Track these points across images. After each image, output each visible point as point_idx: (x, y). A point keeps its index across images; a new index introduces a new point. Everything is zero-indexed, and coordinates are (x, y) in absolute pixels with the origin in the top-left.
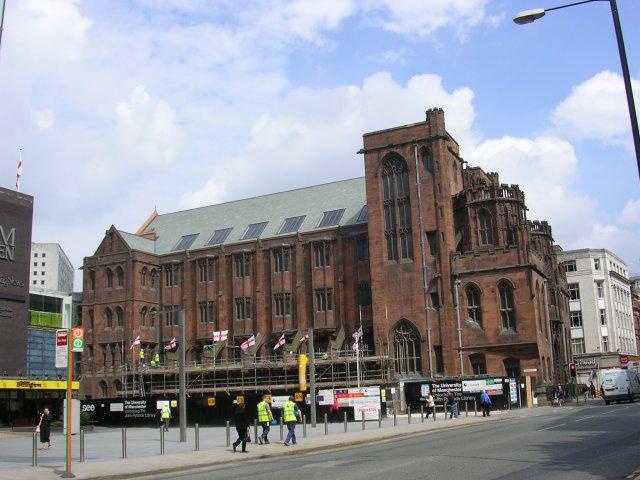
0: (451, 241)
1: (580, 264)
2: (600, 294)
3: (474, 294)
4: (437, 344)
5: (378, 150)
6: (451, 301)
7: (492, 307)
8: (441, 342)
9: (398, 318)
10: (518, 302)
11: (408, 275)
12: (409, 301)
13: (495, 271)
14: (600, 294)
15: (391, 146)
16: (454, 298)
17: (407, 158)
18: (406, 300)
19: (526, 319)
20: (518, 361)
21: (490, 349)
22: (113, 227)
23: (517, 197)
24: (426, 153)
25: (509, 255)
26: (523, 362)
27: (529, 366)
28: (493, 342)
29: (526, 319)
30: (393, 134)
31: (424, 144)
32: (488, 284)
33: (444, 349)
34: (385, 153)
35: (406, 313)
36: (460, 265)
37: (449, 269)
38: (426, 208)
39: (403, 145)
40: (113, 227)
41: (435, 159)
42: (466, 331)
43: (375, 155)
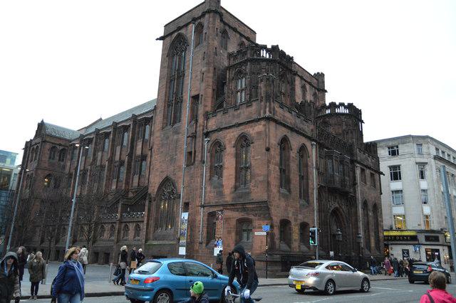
0: (207, 104)
1: (402, 149)
2: (422, 176)
3: (218, 147)
4: (187, 201)
7: (229, 163)
9: (164, 177)
11: (175, 137)
12: (173, 160)
13: (240, 125)
14: (422, 176)
19: (258, 175)
20: (249, 221)
21: (226, 206)
22: (42, 121)
23: (317, 83)
25: (250, 109)
26: (256, 223)
27: (260, 228)
28: (228, 198)
29: (258, 175)
30: (182, 19)
32: (230, 137)
34: (176, 34)
36: (212, 124)
37: (202, 128)
39: (186, 25)
40: (42, 121)
42: (208, 189)
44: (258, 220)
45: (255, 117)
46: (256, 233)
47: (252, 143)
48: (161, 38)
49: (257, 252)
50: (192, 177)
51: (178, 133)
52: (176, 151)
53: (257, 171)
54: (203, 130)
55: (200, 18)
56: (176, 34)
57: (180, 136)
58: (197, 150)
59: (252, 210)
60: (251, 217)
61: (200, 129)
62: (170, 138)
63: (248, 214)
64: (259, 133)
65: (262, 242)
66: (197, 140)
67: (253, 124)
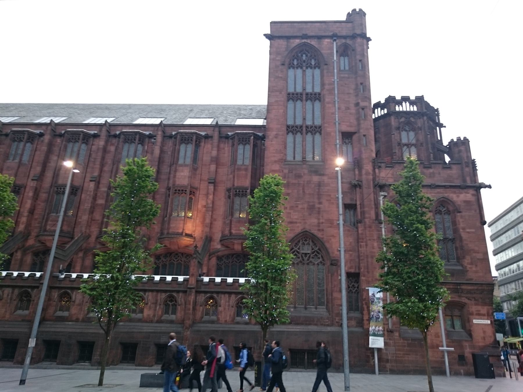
4: (352, 271)
5: (288, 38)
6: (373, 216)
8: (359, 268)
10: (464, 229)
11: (316, 179)
15: (305, 36)
16: (377, 215)
17: (325, 52)
18: (311, 208)
24: (345, 51)
31: (344, 41)
33: (362, 278)
34: (297, 41)
35: (311, 223)
37: (371, 177)
38: (343, 107)
39: (320, 38)
41: (358, 57)
43: (282, 43)
44: (476, 304)
45: (458, 183)
46: (475, 321)
47: (460, 212)
48: (266, 36)
49: (481, 344)
50: (358, 240)
51: (323, 175)
52: (319, 198)
53: (471, 246)
54: (374, 179)
55: (345, 37)
56: (297, 41)
57: (325, 178)
58: (366, 202)
59: (469, 292)
60: (464, 300)
61: (367, 179)
62: (306, 178)
63: (460, 297)
64: (467, 202)
65: (484, 332)
66: (365, 191)
67: (457, 190)
